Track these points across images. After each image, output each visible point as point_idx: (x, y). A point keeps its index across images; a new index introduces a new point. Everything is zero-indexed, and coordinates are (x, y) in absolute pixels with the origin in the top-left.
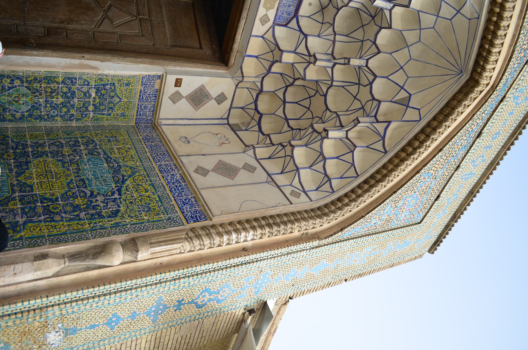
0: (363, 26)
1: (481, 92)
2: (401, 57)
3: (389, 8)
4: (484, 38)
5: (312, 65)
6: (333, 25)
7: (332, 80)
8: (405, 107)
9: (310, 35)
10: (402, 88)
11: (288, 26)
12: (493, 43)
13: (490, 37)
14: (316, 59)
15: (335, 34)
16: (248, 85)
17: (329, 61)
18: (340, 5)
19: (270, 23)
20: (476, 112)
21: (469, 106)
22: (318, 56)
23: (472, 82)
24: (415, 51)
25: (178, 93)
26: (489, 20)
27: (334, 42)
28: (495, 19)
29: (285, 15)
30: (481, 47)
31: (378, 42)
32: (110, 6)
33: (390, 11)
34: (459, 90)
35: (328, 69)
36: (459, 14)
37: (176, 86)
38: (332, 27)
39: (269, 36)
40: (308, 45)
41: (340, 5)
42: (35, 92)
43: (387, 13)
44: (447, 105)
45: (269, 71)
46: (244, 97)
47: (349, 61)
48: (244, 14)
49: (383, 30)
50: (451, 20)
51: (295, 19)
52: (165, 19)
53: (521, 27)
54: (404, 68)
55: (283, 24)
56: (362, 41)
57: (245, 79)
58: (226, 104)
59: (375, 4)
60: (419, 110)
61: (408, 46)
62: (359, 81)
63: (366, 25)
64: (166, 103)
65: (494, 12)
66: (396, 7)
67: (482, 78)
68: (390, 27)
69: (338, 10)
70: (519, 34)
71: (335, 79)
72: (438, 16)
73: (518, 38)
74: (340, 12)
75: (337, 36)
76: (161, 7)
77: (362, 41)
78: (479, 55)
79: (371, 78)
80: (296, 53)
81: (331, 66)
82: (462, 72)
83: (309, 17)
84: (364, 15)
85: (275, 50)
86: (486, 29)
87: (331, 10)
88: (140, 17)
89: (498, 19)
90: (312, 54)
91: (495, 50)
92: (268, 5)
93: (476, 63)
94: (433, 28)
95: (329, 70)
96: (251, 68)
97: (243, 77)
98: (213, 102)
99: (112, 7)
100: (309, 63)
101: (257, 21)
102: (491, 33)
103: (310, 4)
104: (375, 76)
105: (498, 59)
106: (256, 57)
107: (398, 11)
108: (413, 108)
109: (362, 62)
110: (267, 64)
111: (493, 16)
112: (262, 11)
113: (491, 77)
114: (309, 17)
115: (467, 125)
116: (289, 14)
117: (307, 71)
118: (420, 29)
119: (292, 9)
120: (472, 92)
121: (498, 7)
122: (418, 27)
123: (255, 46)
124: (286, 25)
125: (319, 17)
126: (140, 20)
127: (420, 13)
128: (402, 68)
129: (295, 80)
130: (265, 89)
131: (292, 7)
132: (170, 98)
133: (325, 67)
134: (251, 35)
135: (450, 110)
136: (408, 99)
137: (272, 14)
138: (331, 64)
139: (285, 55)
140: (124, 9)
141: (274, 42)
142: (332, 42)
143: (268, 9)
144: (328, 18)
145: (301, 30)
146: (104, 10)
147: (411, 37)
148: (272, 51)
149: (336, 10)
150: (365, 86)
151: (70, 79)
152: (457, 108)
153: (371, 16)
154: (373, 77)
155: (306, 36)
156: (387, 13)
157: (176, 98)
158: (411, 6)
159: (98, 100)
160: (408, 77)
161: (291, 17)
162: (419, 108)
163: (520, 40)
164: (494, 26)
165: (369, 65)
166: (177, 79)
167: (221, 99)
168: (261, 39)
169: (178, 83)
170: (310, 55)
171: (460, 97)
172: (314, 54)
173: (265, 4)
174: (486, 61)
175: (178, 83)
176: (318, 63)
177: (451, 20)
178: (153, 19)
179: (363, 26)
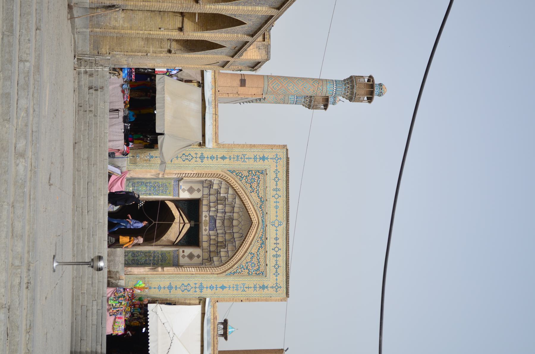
16: (206, 251)
24: (242, 223)
42: (146, 256)
46: (206, 255)
58: (201, 258)
64: (181, 259)
96: (205, 245)
98: (196, 258)
101: (203, 231)
112: (204, 228)
119: (214, 225)
137: (207, 228)
147: (240, 220)
151: (154, 252)
157: (183, 256)
167: (198, 256)
169: (183, 252)
175: (183, 252)
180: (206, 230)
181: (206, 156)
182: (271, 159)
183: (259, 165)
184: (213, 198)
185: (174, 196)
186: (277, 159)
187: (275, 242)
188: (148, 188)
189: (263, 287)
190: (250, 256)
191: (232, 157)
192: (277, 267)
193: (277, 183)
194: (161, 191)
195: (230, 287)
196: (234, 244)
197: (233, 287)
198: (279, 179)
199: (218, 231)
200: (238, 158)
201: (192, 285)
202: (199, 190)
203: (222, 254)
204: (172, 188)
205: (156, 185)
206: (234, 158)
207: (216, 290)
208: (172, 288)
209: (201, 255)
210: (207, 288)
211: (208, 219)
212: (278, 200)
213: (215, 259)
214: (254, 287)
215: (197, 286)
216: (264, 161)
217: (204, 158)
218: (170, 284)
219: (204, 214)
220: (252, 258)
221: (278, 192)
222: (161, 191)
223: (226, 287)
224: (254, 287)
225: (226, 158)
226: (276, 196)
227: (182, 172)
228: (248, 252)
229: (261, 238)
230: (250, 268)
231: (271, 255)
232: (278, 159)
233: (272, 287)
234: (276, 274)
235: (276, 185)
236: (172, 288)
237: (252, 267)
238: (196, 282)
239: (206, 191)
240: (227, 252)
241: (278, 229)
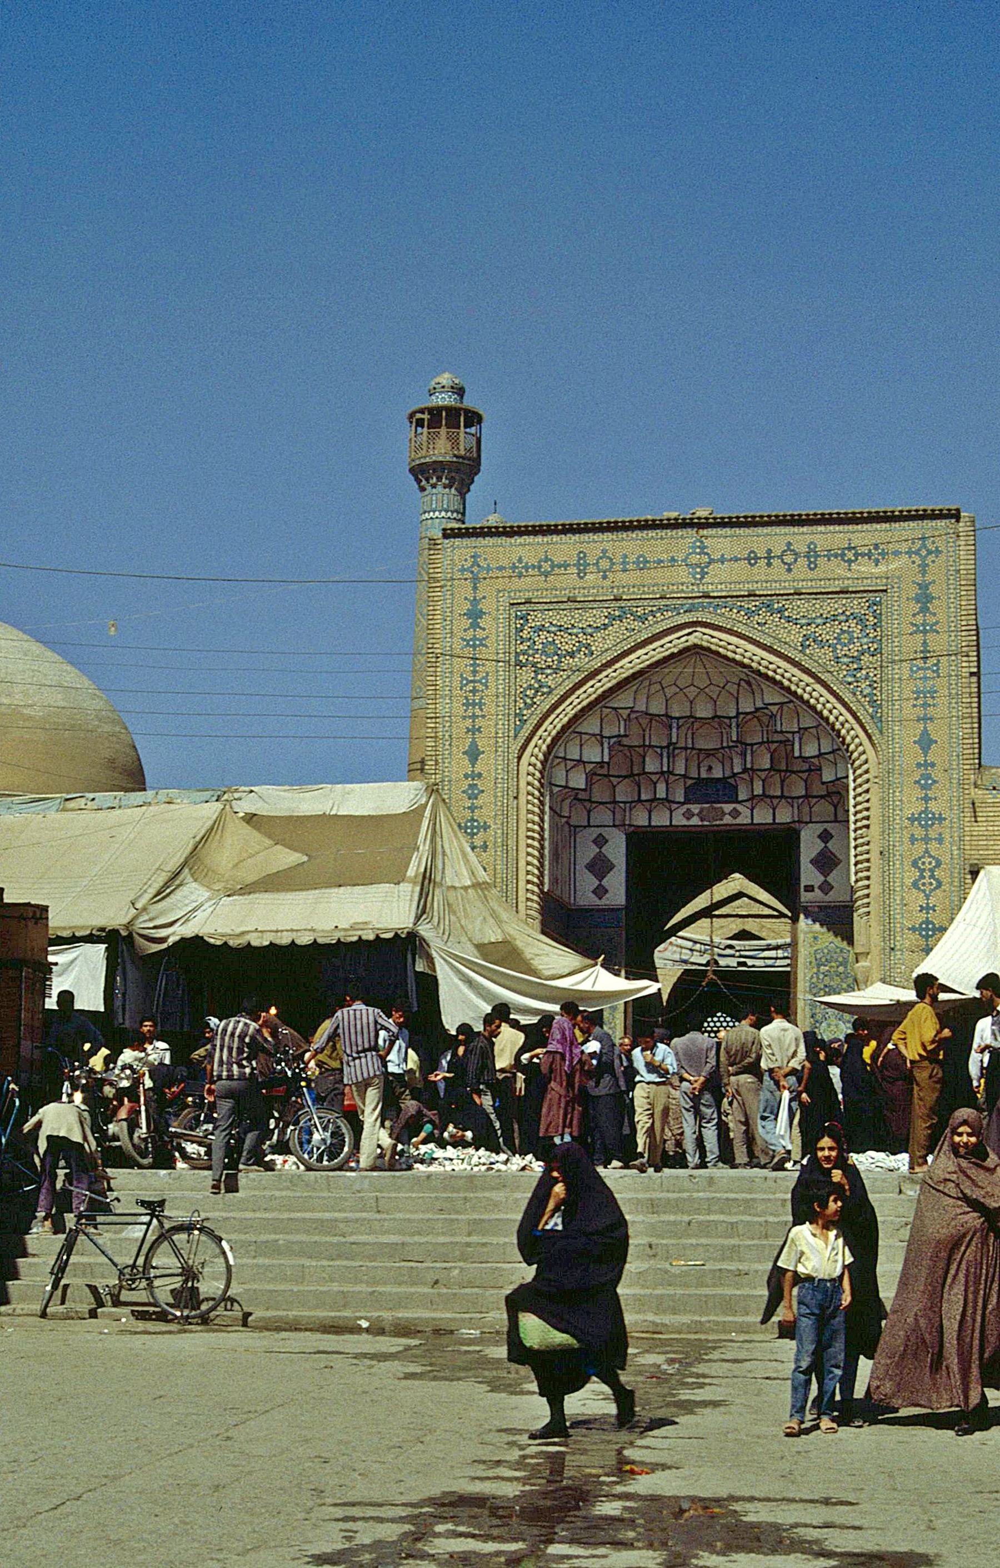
7: (763, 742)
16: (806, 809)
19: (739, 807)
25: (820, 888)
37: (813, 891)
45: (782, 797)
46: (823, 808)
57: (796, 819)
96: (785, 816)
97: (794, 822)
101: (738, 821)
106: (774, 809)
110: (775, 801)
112: (728, 820)
123: (763, 816)
129: (780, 771)
130: (803, 793)
132: (826, 894)
134: (752, 824)
137: (728, 808)
143: (724, 814)
159: (833, 964)
166: (805, 891)
169: (809, 889)
175: (809, 889)
180: (735, 814)
181: (468, 814)
182: (475, 588)
183: (496, 628)
184: (624, 792)
186: (475, 569)
187: (763, 562)
189: (924, 599)
190: (814, 650)
191: (469, 723)
192: (850, 555)
193: (559, 567)
195: (925, 719)
196: (774, 709)
197: (925, 705)
198: (546, 560)
199: (737, 769)
200: (474, 704)
201: (919, 848)
202: (600, 841)
203: (810, 750)
206: (474, 717)
207: (933, 765)
208: (927, 922)
209: (819, 828)
210: (926, 799)
211: (695, 808)
212: (618, 559)
213: (828, 776)
214: (925, 632)
215: (919, 833)
216: (481, 614)
217: (473, 820)
218: (913, 929)
219: (679, 820)
220: (821, 644)
221: (591, 560)
223: (925, 732)
224: (925, 632)
225: (474, 744)
226: (604, 564)
228: (798, 657)
229: (750, 614)
230: (854, 649)
231: (811, 575)
232: (475, 564)
233: (924, 568)
234: (877, 554)
235: (566, 566)
236: (927, 922)
237: (851, 641)
238: (906, 840)
239: (602, 816)
240: (802, 730)
241: (717, 556)
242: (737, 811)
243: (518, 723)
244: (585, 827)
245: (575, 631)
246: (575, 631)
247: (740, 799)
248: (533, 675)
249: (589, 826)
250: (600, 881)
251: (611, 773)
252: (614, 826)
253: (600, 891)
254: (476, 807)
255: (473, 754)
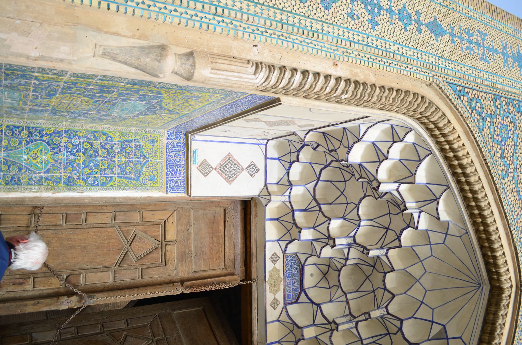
0: (367, 277)
1: (510, 296)
2: (416, 292)
3: (384, 253)
4: (482, 247)
5: (335, 331)
6: (340, 286)
8: (446, 340)
9: (322, 303)
10: (432, 322)
11: (299, 301)
12: (492, 248)
13: (487, 244)
14: (337, 325)
15: (345, 294)
17: (350, 321)
18: (339, 267)
19: (281, 305)
20: (517, 317)
21: (506, 314)
22: (338, 321)
23: (496, 292)
26: (477, 231)
27: (347, 301)
28: (482, 228)
29: (293, 293)
30: (484, 255)
31: (388, 287)
32: (126, 336)
33: (386, 255)
34: (488, 303)
35: (352, 330)
36: (448, 236)
38: (340, 289)
39: (284, 317)
40: (324, 313)
41: (339, 267)
43: (384, 258)
44: (485, 322)
47: (369, 315)
48: (254, 305)
49: (387, 274)
50: (444, 243)
51: (303, 293)
52: (180, 333)
53: (509, 225)
54: (424, 301)
55: (293, 301)
56: (373, 291)
59: (370, 255)
60: (460, 338)
61: (418, 280)
62: (388, 330)
63: (370, 275)
65: (478, 223)
66: (390, 250)
67: (503, 284)
68: (393, 270)
69: (339, 271)
70: (511, 232)
71: (363, 337)
72: (431, 245)
73: (512, 235)
74: (342, 272)
75: (348, 295)
76: (174, 322)
77: (373, 291)
78: (487, 264)
79: (398, 323)
80: (315, 325)
81: (354, 326)
82: (480, 285)
83: (315, 287)
84: (364, 268)
85: (294, 328)
86: (479, 239)
87: (333, 274)
88: (157, 338)
89: (484, 227)
90: (331, 320)
91: (498, 254)
92: (274, 289)
93: (489, 271)
94: (432, 255)
95: (354, 330)
99: (128, 337)
100: (332, 330)
101: (269, 308)
102: (486, 241)
103: (312, 275)
104: (401, 321)
105: (506, 260)
107: (391, 253)
108: (454, 338)
109: (383, 311)
111: (479, 226)
112: (270, 297)
113: (510, 279)
114: (315, 287)
115: (517, 334)
116: (296, 291)
117: (332, 339)
118: (421, 261)
119: (297, 285)
120: (501, 300)
121: (478, 218)
122: (418, 261)
124: (296, 302)
125: (323, 284)
126: (156, 341)
127: (413, 247)
128: (422, 302)
131: (296, 284)
133: (349, 329)
135: (490, 326)
136: (443, 331)
137: (280, 296)
138: (353, 324)
139: (305, 331)
140: (140, 336)
141: (290, 321)
142: (345, 302)
143: (275, 293)
144: (333, 281)
145: (312, 302)
146: (121, 343)
147: (416, 271)
148: (292, 331)
149: (338, 272)
150: (396, 334)
152: (497, 322)
153: (371, 266)
154: (399, 322)
155: (319, 305)
156: (384, 258)
158: (403, 245)
160: (433, 309)
161: (298, 292)
162: (460, 336)
163: (514, 236)
164: (485, 234)
165: (390, 312)
168: (277, 323)
170: (330, 323)
171: (493, 310)
172: (333, 320)
173: (270, 289)
174: (497, 266)
176: (341, 328)
177: (444, 243)
178: (168, 337)
179: (367, 277)
180: (274, 305)
185: (168, 188)
188: (63, 156)
194: (117, 170)
202: (252, 169)
204: (162, 161)
205: (97, 144)
211: (279, 265)
222: (117, 170)
227: (289, 62)
242: (277, 305)
243: (459, 88)
244: (266, 156)
245: (515, 161)
246: (515, 161)
247: (288, 307)
248: (489, 112)
249: (266, 158)
250: (215, 169)
251: (320, 182)
252: (266, 185)
253: (205, 168)
254: (391, 17)
255: (435, 28)
